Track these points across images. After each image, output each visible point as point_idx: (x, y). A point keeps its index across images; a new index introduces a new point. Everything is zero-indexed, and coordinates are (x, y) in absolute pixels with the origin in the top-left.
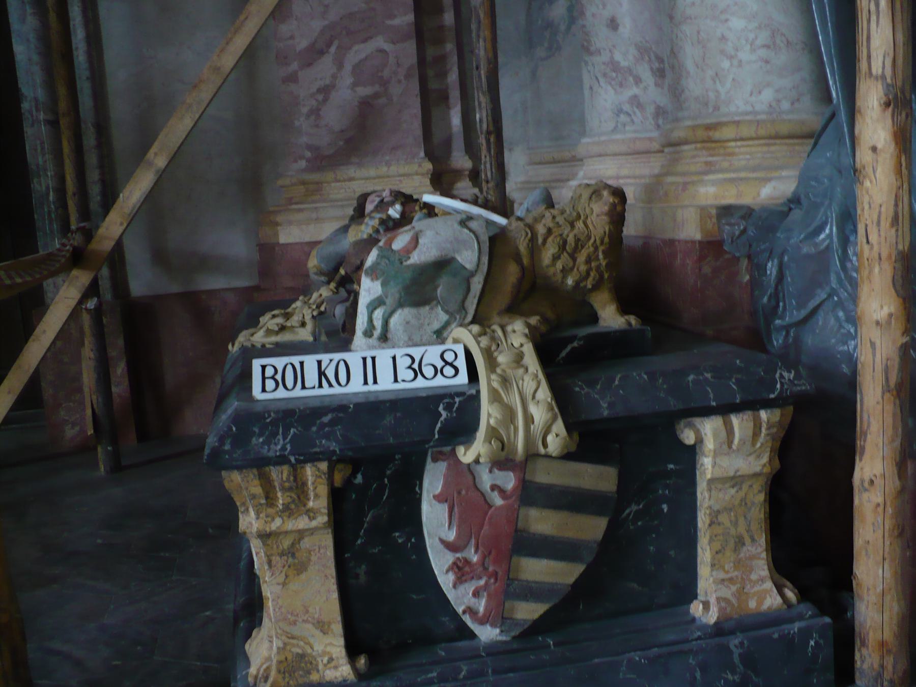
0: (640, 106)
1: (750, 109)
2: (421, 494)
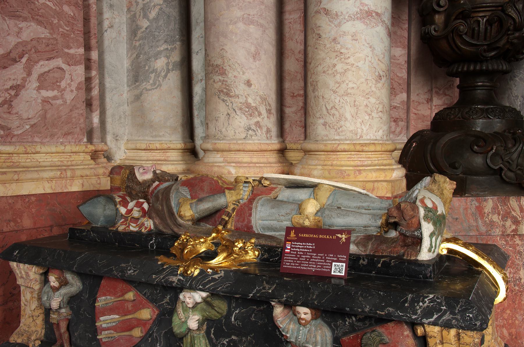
0: (260, 127)
1: (375, 138)
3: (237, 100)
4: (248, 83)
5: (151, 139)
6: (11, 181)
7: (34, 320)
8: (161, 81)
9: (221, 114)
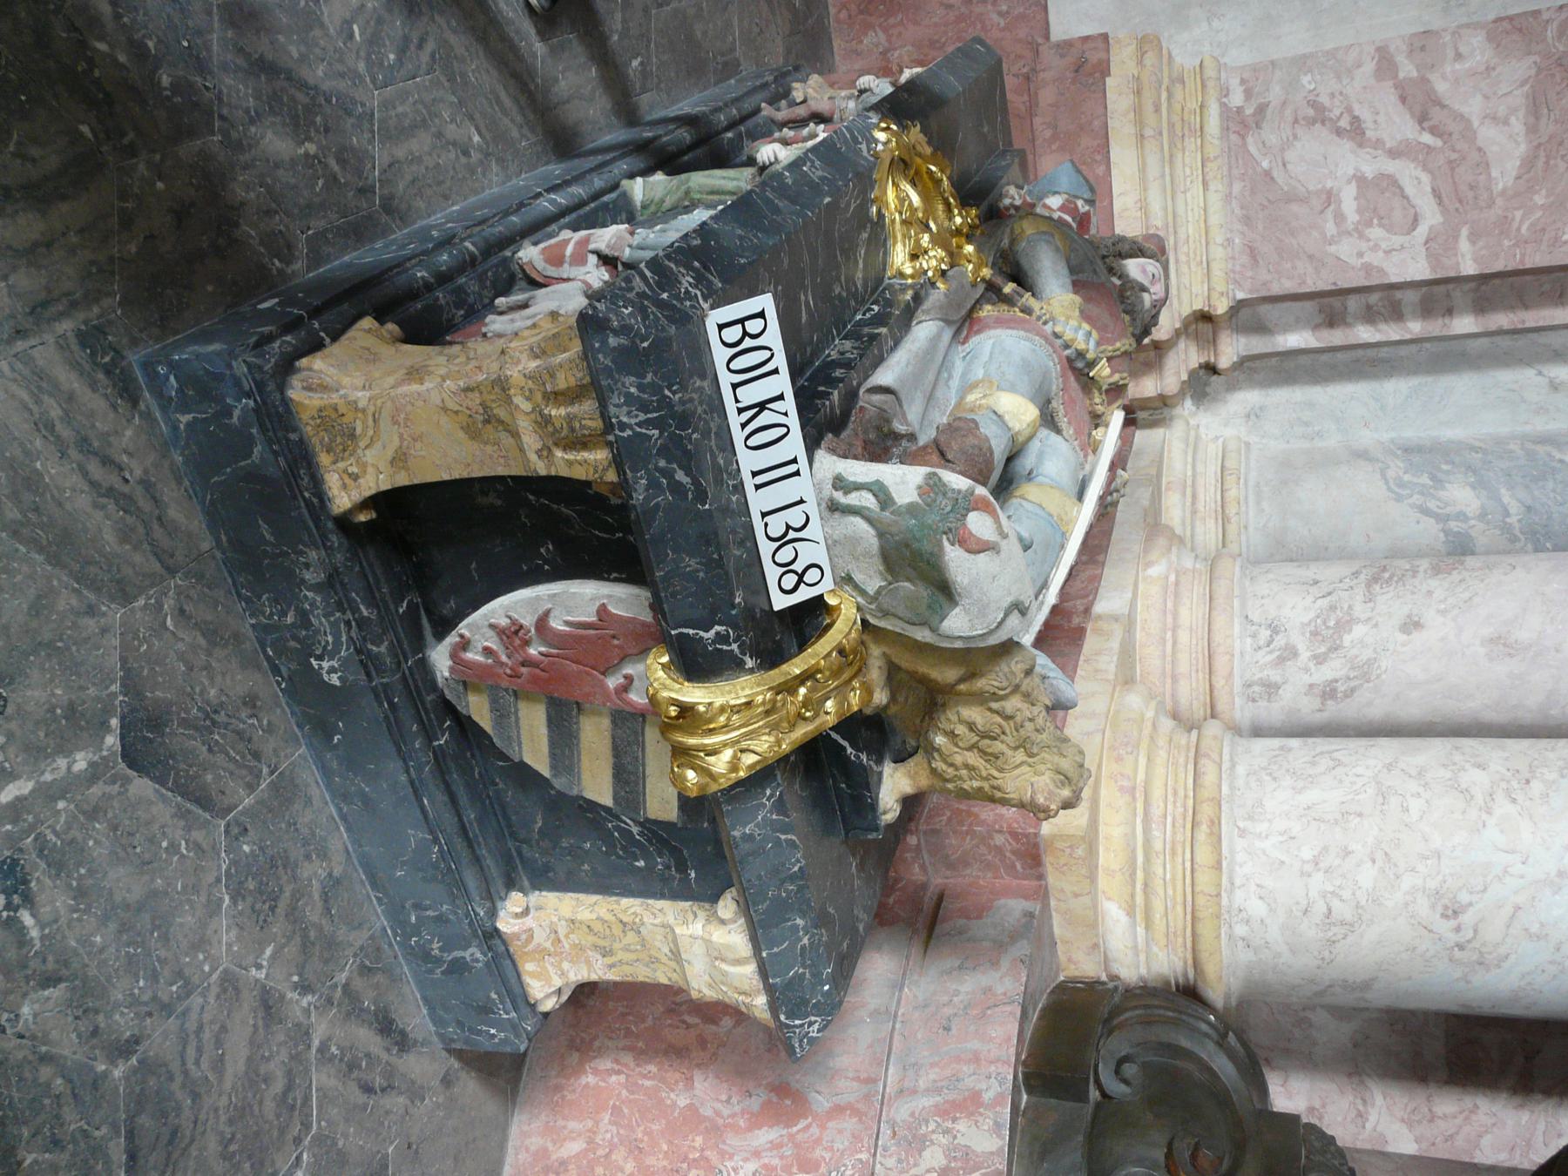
0: (1281, 661)
1: (1238, 882)
2: (608, 580)
3: (1360, 598)
4: (1412, 625)
5: (1251, 483)
6: (1140, 123)
8: (1410, 501)
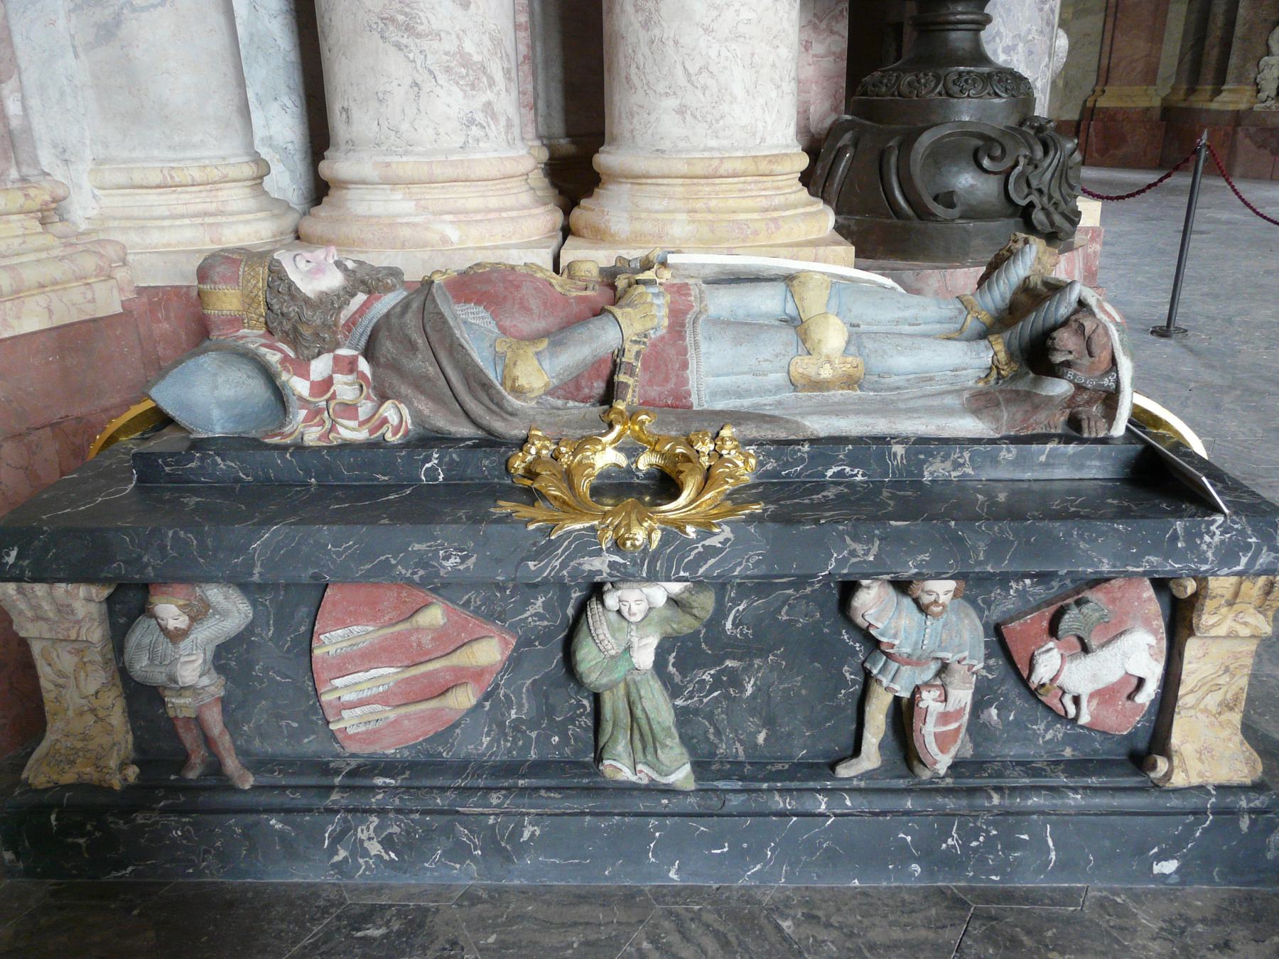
0: (494, 116)
3: (435, 44)
5: (171, 155)
7: (99, 719)
9: (395, 83)
